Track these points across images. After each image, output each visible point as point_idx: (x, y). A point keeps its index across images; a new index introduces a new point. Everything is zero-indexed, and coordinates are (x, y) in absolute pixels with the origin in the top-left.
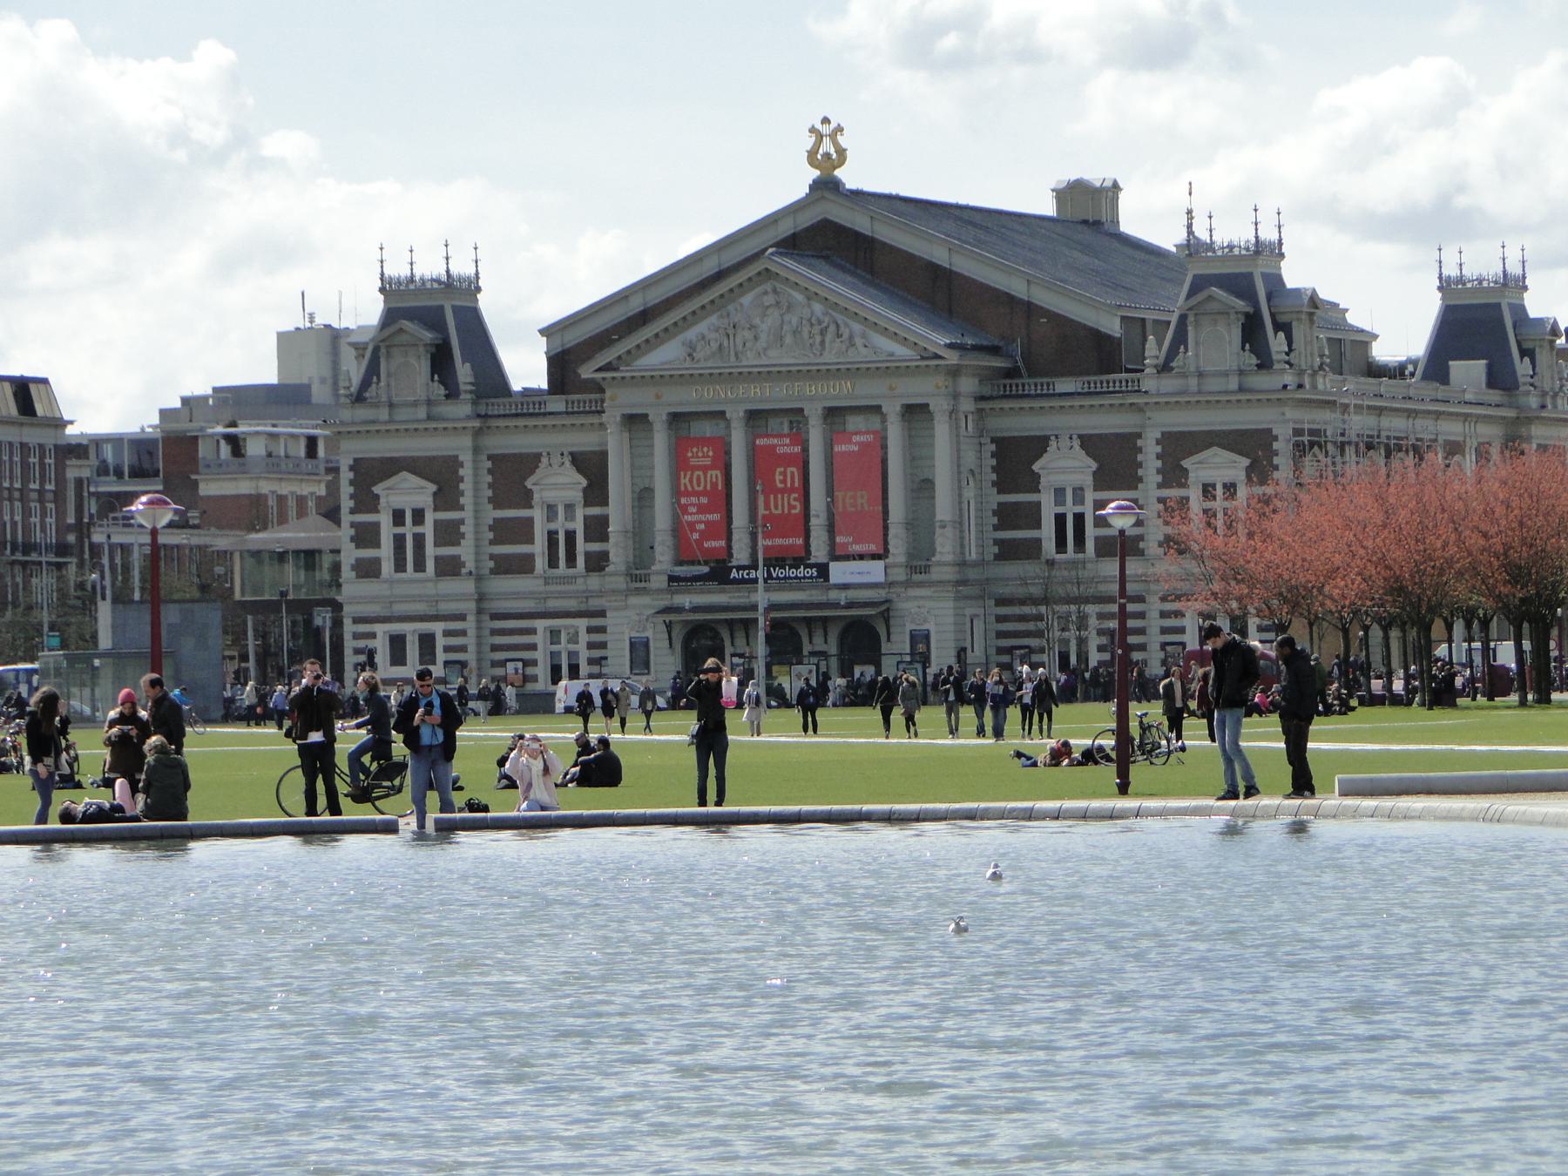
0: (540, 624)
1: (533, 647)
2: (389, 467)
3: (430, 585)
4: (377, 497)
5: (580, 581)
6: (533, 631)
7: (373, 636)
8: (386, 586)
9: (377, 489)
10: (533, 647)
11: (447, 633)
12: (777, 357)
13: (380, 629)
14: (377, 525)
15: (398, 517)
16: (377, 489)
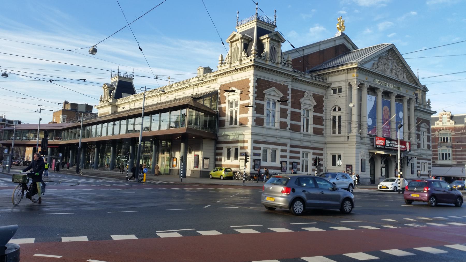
0: (301, 150)
1: (299, 158)
2: (268, 84)
3: (278, 131)
4: (264, 94)
5: (312, 137)
6: (299, 153)
7: (259, 149)
8: (265, 129)
9: (264, 92)
10: (299, 158)
11: (282, 151)
12: (390, 76)
13: (262, 146)
14: (263, 105)
15: (268, 103)
16: (264, 92)
